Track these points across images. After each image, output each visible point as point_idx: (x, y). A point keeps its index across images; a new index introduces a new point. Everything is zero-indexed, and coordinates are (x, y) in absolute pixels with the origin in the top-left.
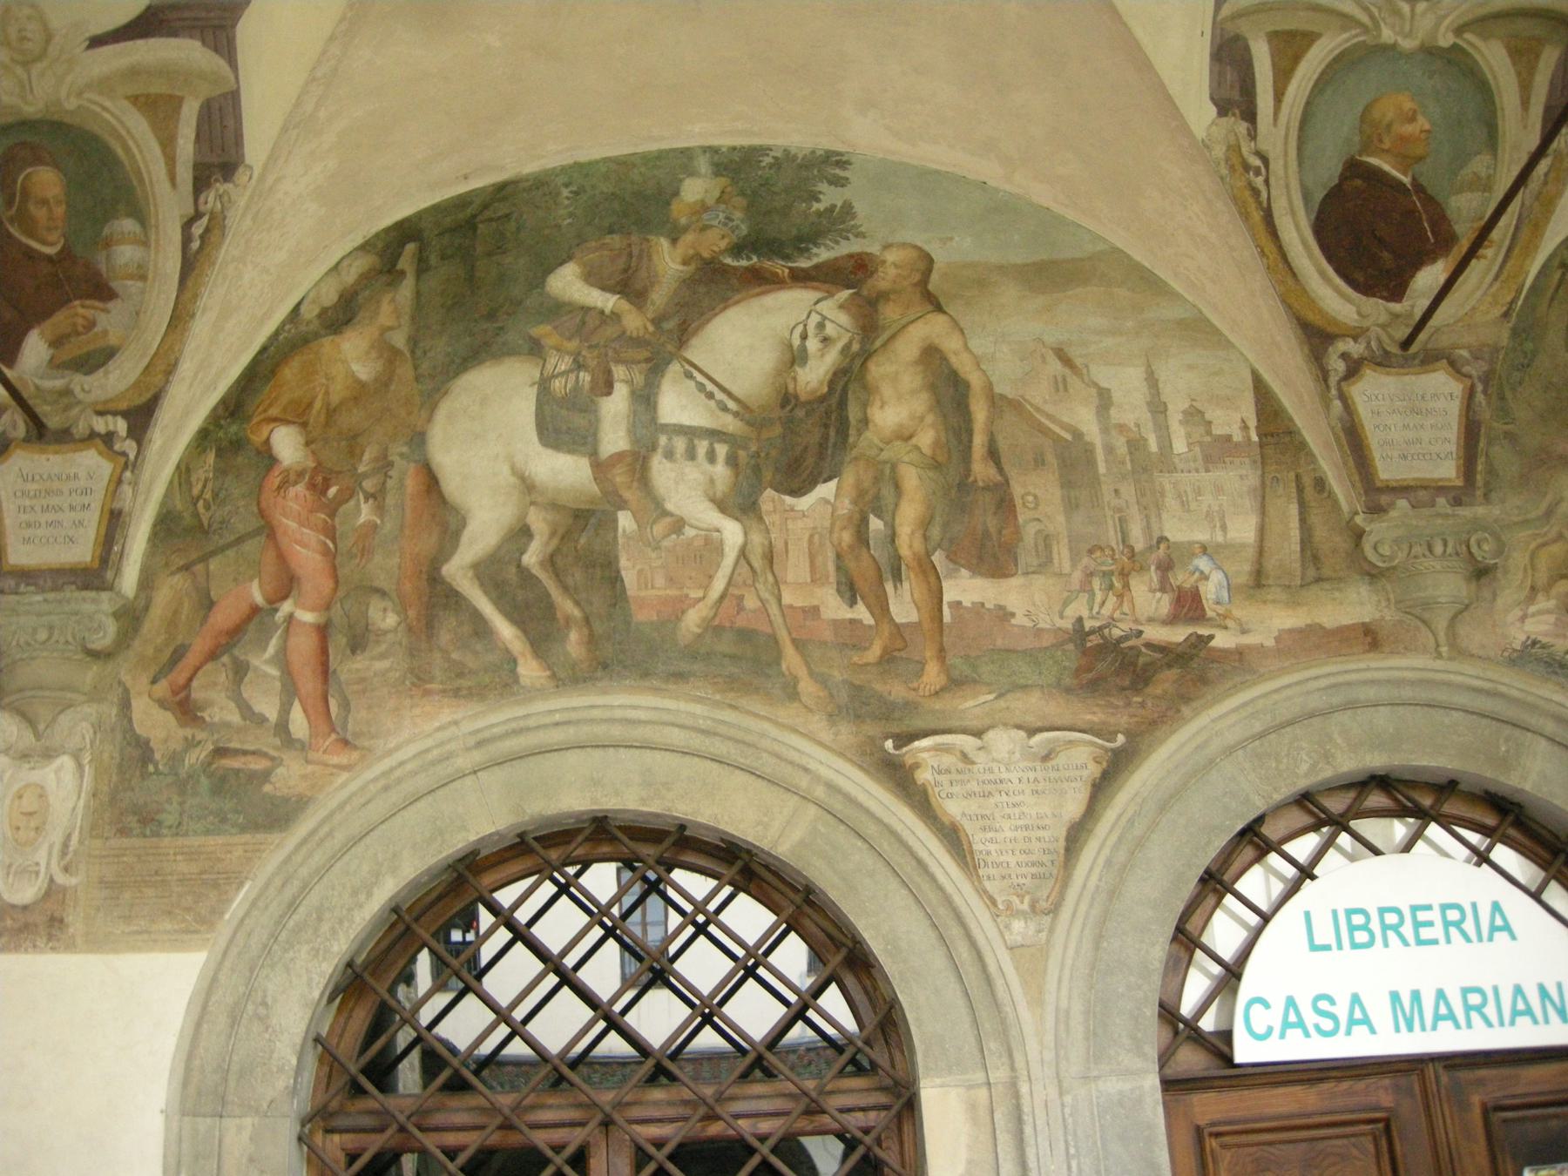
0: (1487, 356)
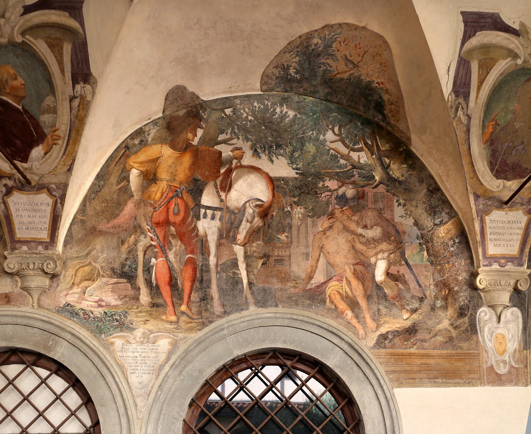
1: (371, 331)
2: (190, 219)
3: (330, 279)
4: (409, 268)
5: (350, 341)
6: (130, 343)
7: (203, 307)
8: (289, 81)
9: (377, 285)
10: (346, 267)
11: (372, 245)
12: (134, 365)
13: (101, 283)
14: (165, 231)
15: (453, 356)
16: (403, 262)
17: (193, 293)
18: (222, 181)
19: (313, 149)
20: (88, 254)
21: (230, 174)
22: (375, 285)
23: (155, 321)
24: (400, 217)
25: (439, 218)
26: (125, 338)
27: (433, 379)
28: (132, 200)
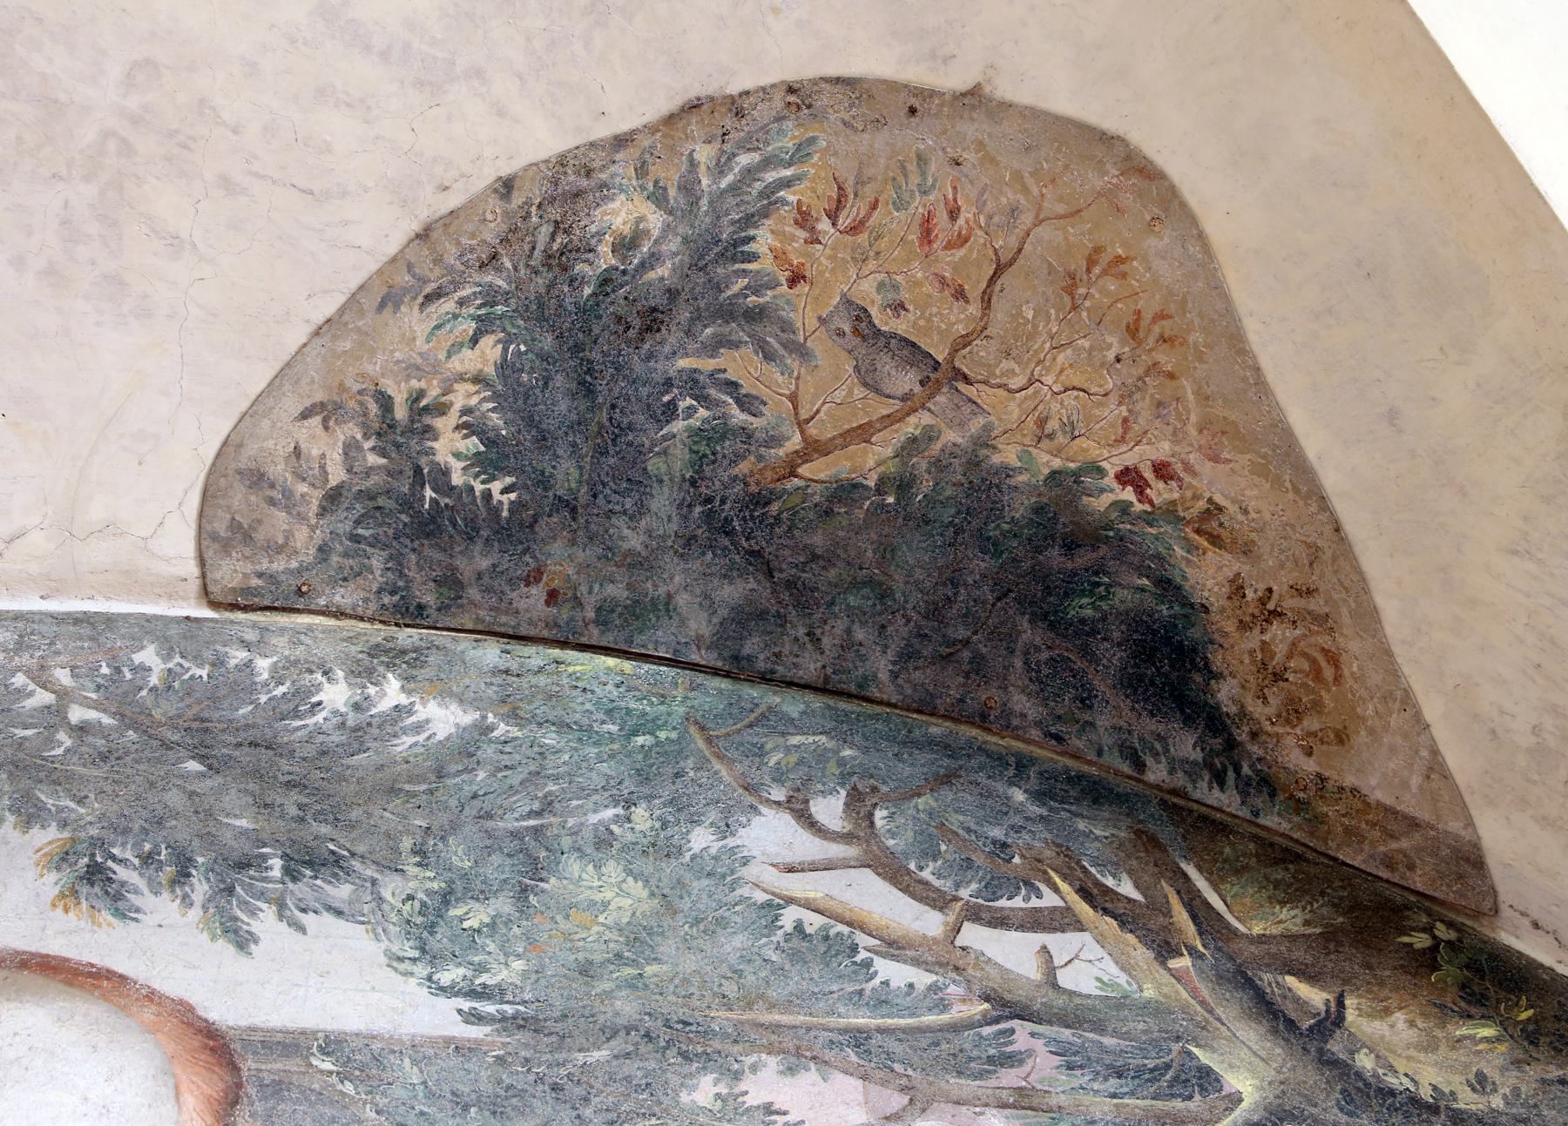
8: (428, 526)
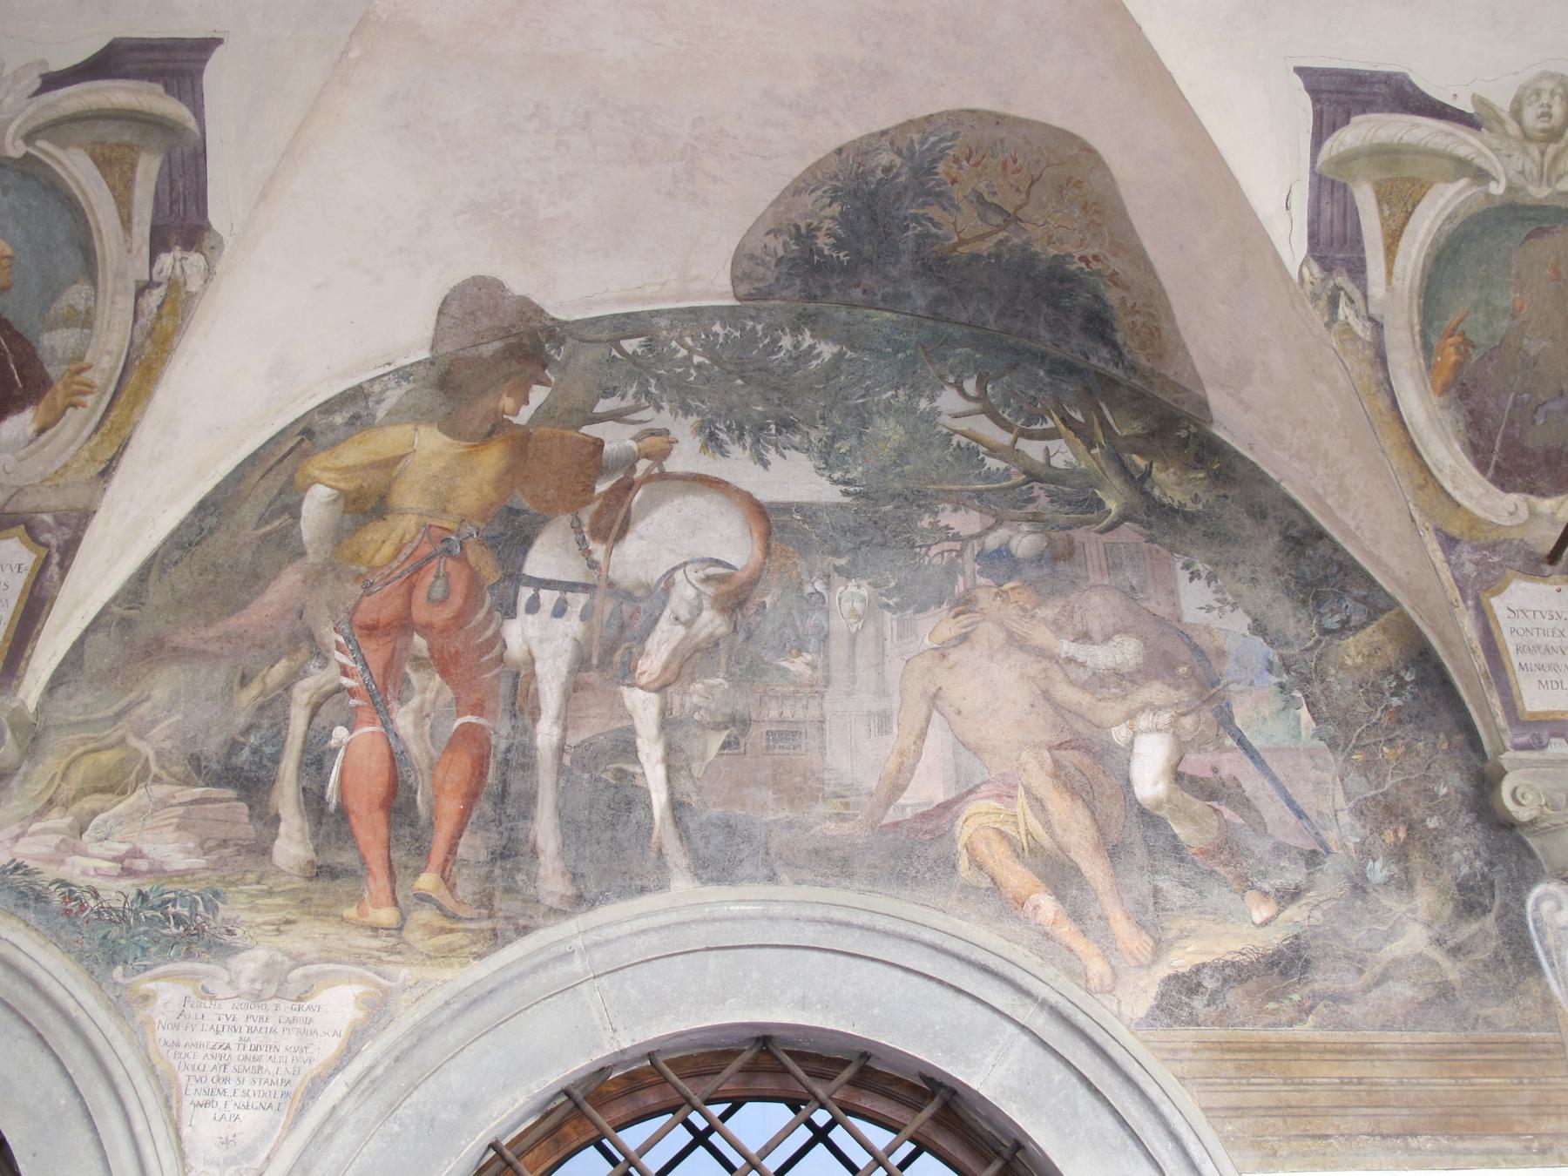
0: (73, 522)
1: (1133, 963)
2: (480, 616)
3: (970, 792)
4: (1252, 758)
5: (1054, 998)
6: (213, 998)
7: (499, 881)
9: (1143, 812)
10: (1025, 756)
11: (1113, 690)
12: (214, 1073)
13: (145, 801)
14: (394, 649)
15: (1464, 1051)
16: (1229, 742)
17: (466, 834)
18: (599, 514)
19: (896, 433)
20: (119, 715)
21: (627, 494)
22: (1135, 811)
23: (317, 924)
24: (1201, 608)
25: (1334, 613)
26: (198, 981)
27: (1398, 1136)
28: (299, 564)
